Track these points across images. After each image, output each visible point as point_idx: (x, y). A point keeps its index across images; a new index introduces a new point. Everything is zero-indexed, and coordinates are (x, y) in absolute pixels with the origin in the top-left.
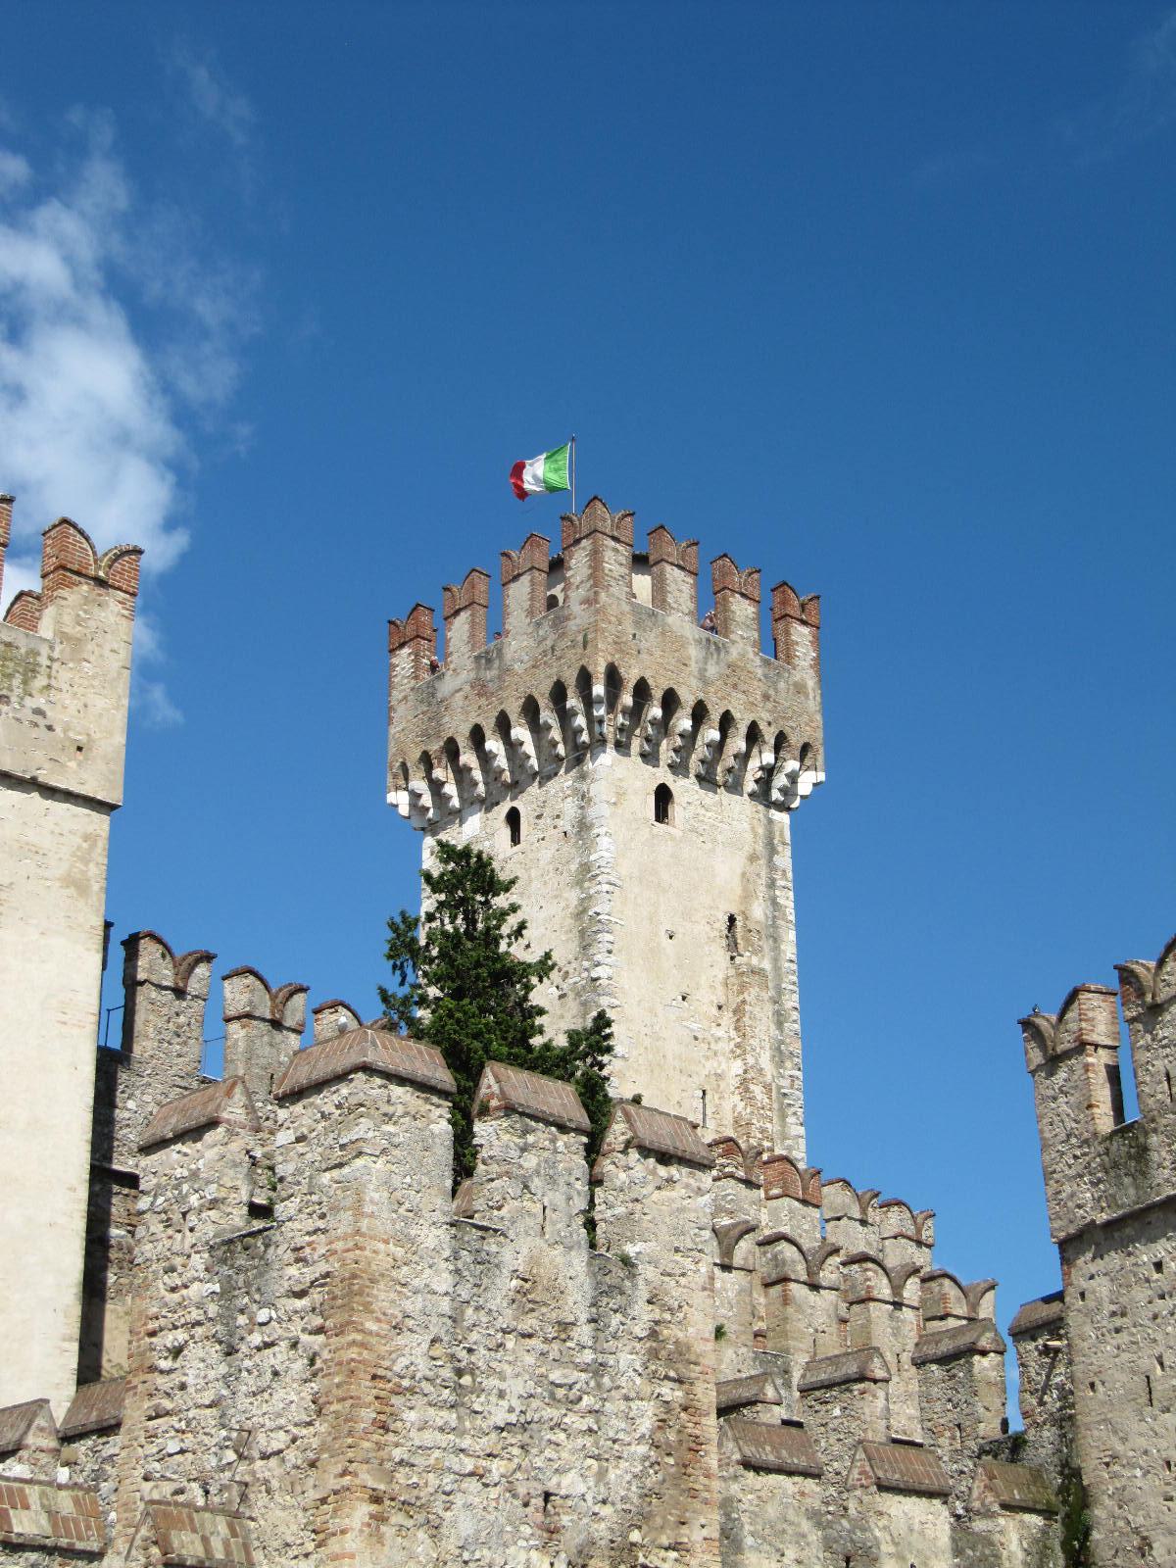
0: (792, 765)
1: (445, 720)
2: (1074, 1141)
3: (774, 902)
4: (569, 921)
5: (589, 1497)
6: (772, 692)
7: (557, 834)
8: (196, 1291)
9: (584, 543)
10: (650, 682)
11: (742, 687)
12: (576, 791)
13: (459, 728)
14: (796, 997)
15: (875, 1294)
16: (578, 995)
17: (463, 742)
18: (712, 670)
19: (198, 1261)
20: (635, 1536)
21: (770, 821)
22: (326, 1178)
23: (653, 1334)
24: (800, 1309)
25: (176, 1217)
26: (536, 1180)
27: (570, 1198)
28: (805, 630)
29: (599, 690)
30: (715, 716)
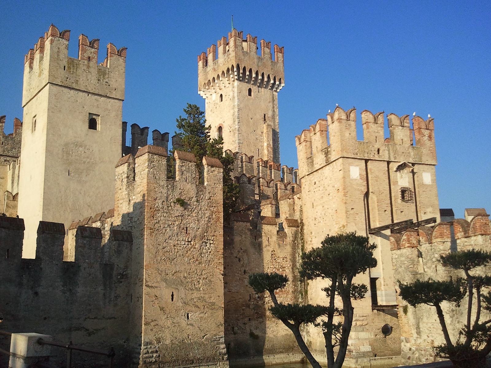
1: (208, 76)
2: (303, 159)
3: (274, 111)
4: (231, 117)
6: (273, 68)
8: (124, 193)
9: (232, 38)
11: (267, 67)
16: (233, 131)
17: (211, 81)
18: (260, 64)
20: (205, 234)
21: (273, 95)
23: (210, 199)
25: (121, 180)
26: (185, 172)
29: (235, 69)
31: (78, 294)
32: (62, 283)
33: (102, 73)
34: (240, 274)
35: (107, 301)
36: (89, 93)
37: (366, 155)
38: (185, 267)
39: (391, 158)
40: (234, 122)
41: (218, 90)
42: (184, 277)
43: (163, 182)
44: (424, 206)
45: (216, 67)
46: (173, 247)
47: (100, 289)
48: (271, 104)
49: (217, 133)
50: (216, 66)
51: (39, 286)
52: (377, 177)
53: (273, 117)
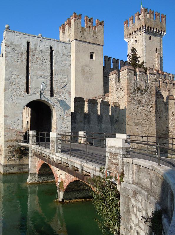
17: (131, 34)
22: (124, 78)
29: (144, 27)
31: (103, 127)
32: (97, 123)
33: (95, 33)
35: (112, 130)
40: (143, 53)
41: (134, 38)
45: (134, 27)
47: (110, 125)
48: (159, 43)
50: (134, 26)
51: (90, 124)
53: (160, 49)
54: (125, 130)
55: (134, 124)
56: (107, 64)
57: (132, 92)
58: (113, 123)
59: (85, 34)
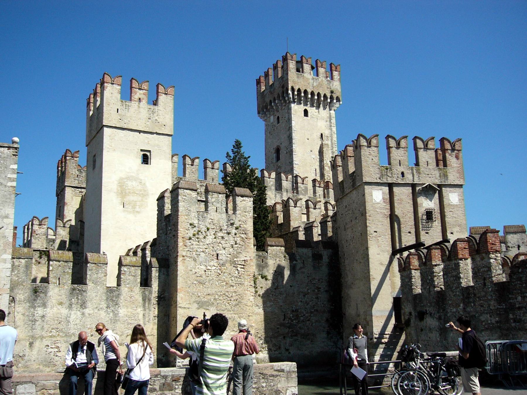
0: (335, 101)
3: (331, 129)
5: (226, 254)
6: (329, 87)
7: (285, 121)
10: (301, 89)
12: (288, 111)
13: (267, 100)
14: (336, 148)
15: (329, 209)
19: (163, 219)
20: (235, 259)
24: (312, 213)
27: (222, 205)
28: (337, 72)
29: (290, 92)
30: (316, 94)
31: (120, 315)
32: (106, 306)
34: (275, 295)
35: (147, 319)
36: (140, 132)
37: (389, 179)
38: (216, 290)
39: (415, 180)
42: (215, 299)
43: (194, 214)
44: (450, 226)
46: (204, 272)
47: (140, 310)
48: (328, 123)
49: (275, 155)
51: (86, 308)
52: (401, 200)
54: (175, 319)
55: (196, 305)
56: (187, 172)
57: (192, 236)
58: (149, 304)
59: (128, 114)
